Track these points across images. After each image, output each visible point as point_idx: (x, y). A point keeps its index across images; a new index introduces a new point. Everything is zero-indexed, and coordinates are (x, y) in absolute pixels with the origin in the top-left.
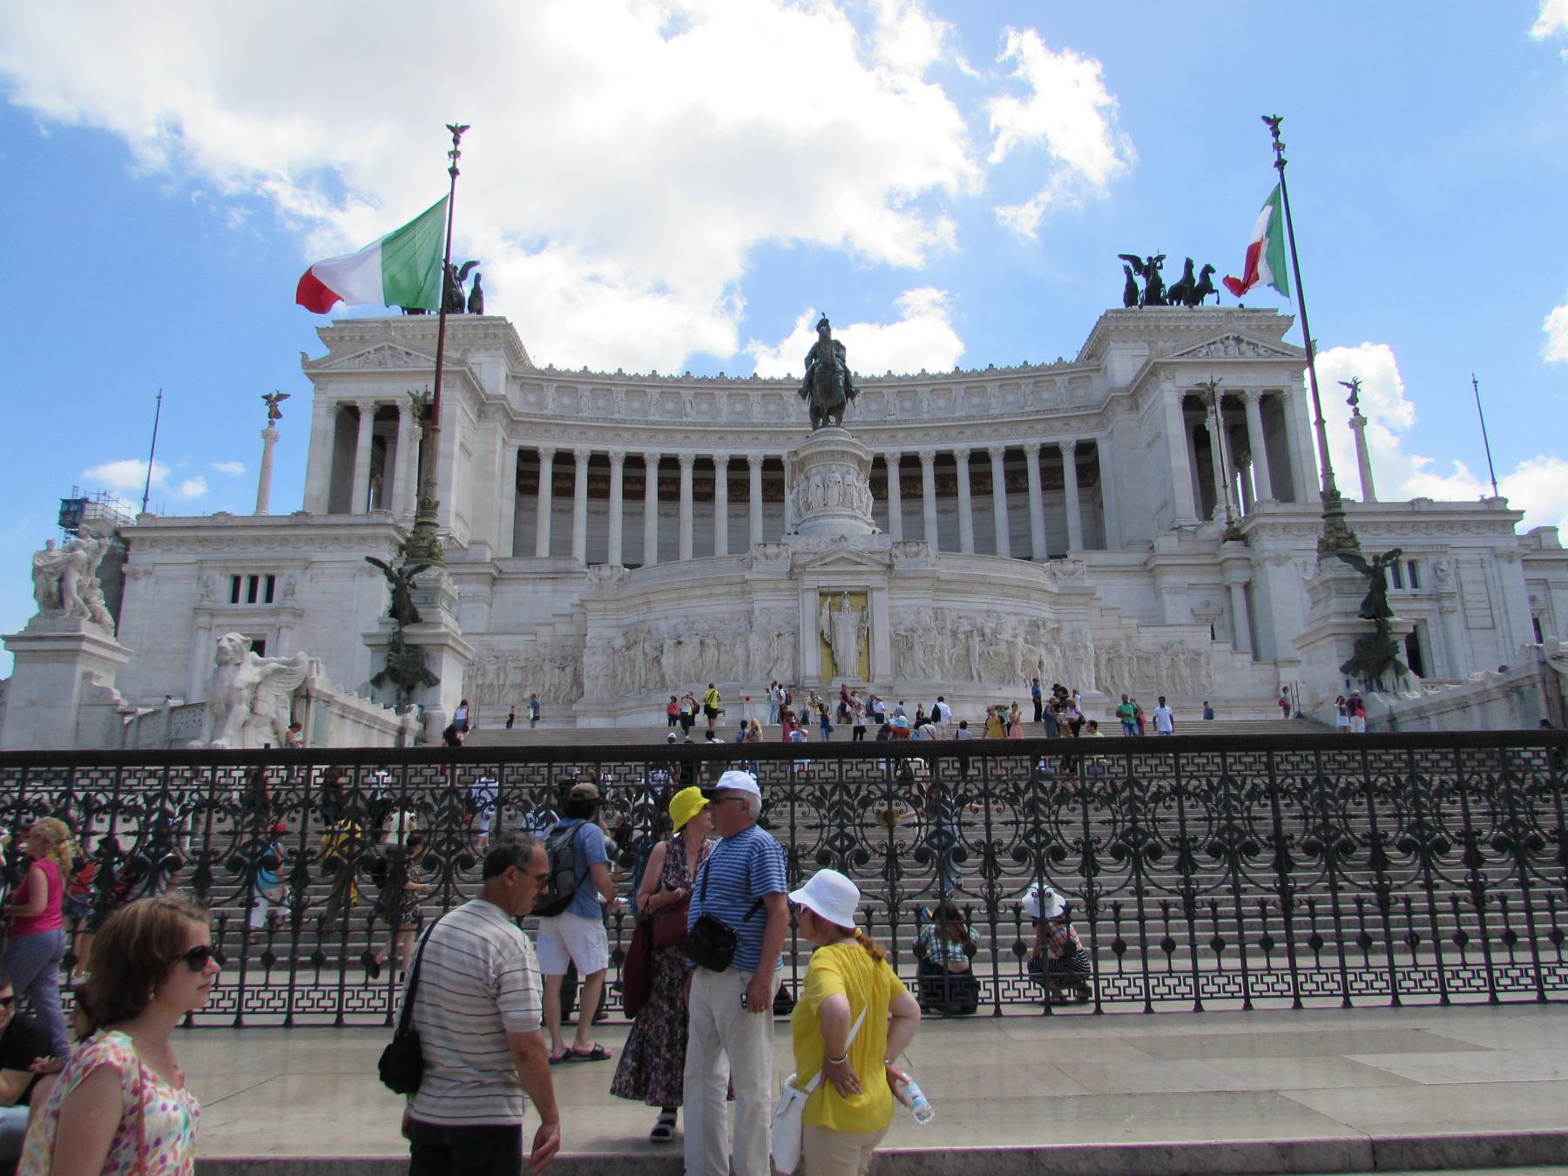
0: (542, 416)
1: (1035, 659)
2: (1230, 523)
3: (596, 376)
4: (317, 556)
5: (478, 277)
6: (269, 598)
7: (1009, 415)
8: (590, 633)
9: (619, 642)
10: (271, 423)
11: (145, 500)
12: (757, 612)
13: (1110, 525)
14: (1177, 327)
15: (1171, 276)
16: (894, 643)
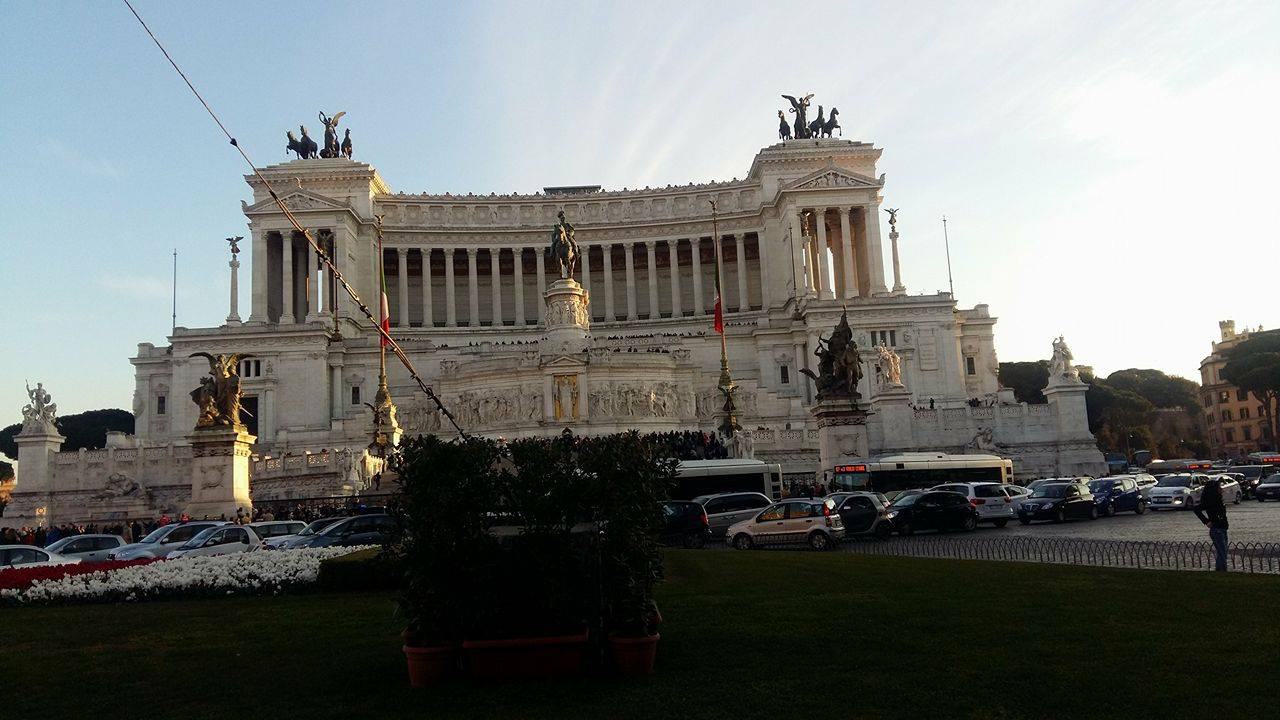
0: (398, 228)
1: (662, 403)
2: (797, 310)
3: (431, 198)
4: (284, 349)
5: (348, 131)
6: (258, 373)
7: (702, 217)
8: (443, 395)
9: (458, 400)
10: (235, 257)
11: (174, 316)
12: (524, 386)
13: (765, 289)
14: (806, 159)
15: (811, 116)
16: (589, 399)
